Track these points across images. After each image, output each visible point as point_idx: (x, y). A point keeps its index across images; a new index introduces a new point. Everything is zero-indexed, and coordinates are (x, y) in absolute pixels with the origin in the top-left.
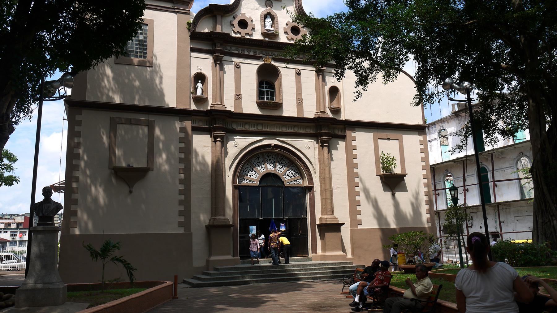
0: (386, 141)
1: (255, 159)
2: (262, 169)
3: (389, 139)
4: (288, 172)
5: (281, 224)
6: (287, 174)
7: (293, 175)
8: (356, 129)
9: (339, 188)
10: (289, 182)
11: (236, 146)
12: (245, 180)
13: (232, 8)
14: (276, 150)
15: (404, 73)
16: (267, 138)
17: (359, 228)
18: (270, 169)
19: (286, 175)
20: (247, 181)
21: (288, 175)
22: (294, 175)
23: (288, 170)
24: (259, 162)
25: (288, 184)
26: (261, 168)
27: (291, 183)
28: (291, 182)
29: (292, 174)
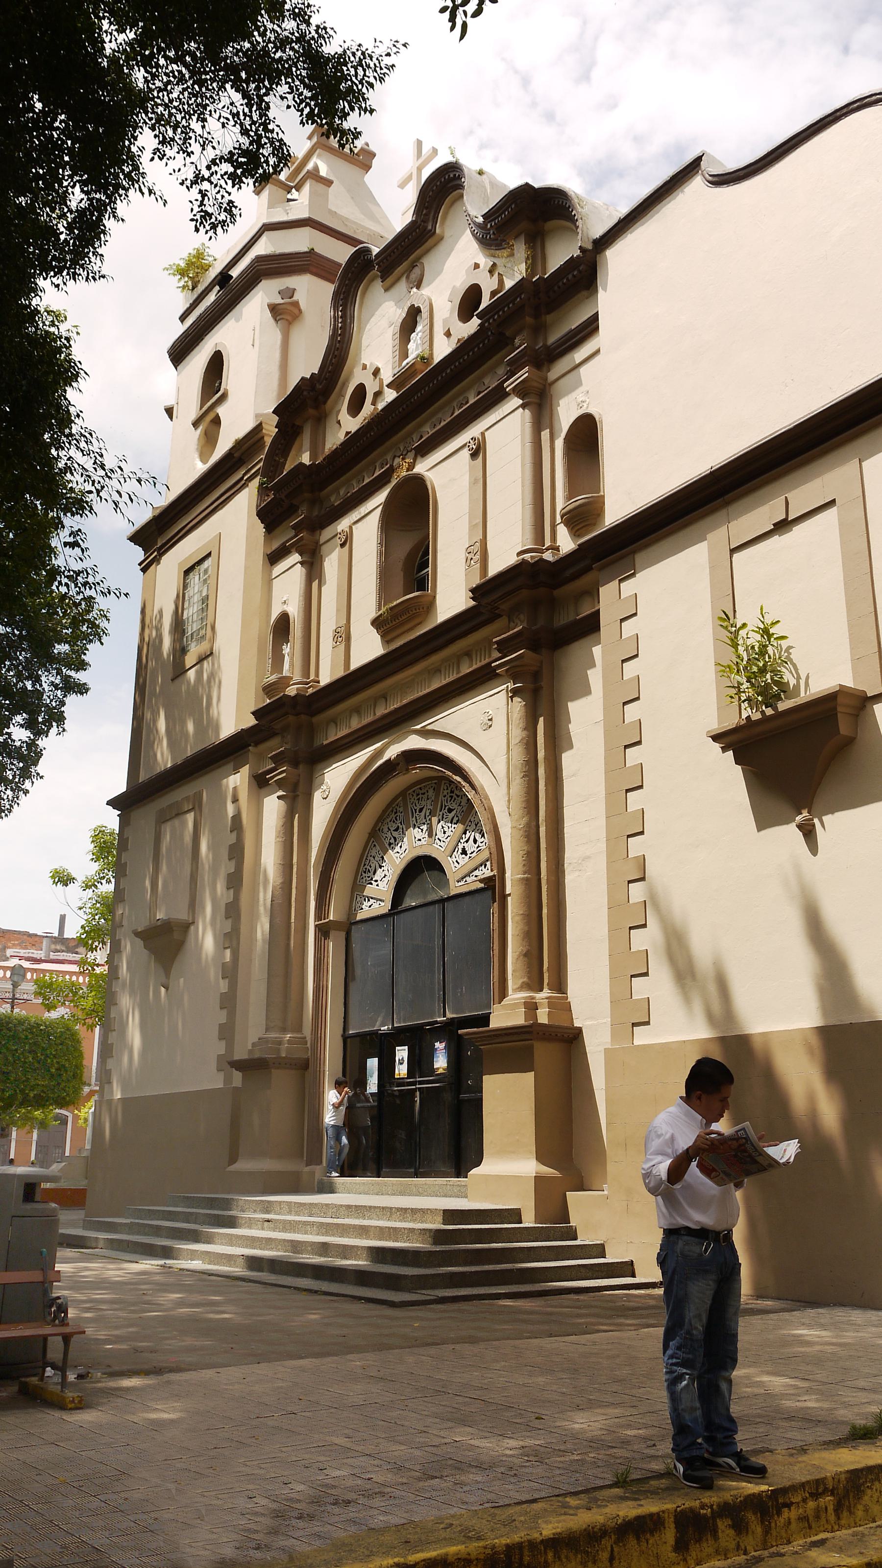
0: (775, 539)
1: (388, 820)
2: (403, 848)
3: (782, 526)
4: (464, 840)
5: (437, 1045)
6: (460, 846)
7: (477, 845)
8: (639, 558)
9: (589, 857)
10: (463, 878)
11: (325, 798)
12: (365, 900)
13: (326, 379)
14: (417, 772)
15: (846, 115)
16: (395, 736)
17: (636, 1042)
18: (419, 843)
19: (460, 851)
20: (370, 903)
21: (464, 852)
22: (478, 846)
23: (465, 833)
24: (396, 830)
25: (460, 884)
26: (401, 847)
27: (469, 879)
28: (468, 875)
29: (475, 841)
